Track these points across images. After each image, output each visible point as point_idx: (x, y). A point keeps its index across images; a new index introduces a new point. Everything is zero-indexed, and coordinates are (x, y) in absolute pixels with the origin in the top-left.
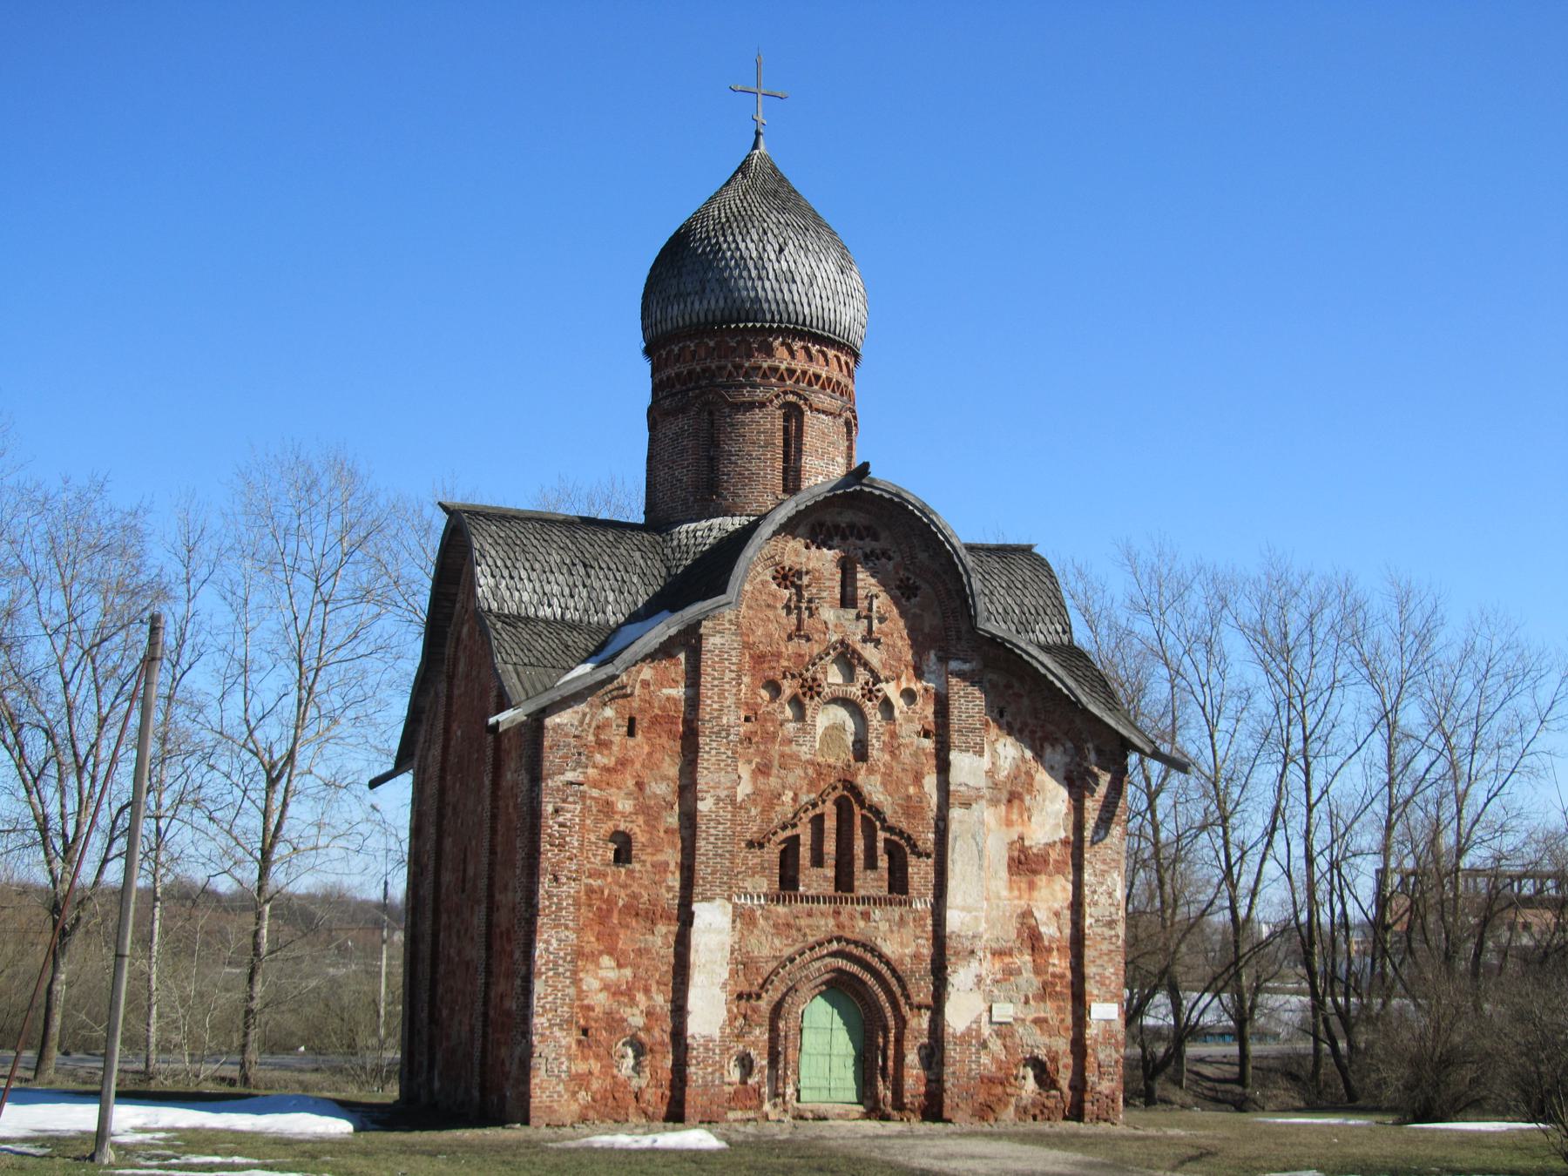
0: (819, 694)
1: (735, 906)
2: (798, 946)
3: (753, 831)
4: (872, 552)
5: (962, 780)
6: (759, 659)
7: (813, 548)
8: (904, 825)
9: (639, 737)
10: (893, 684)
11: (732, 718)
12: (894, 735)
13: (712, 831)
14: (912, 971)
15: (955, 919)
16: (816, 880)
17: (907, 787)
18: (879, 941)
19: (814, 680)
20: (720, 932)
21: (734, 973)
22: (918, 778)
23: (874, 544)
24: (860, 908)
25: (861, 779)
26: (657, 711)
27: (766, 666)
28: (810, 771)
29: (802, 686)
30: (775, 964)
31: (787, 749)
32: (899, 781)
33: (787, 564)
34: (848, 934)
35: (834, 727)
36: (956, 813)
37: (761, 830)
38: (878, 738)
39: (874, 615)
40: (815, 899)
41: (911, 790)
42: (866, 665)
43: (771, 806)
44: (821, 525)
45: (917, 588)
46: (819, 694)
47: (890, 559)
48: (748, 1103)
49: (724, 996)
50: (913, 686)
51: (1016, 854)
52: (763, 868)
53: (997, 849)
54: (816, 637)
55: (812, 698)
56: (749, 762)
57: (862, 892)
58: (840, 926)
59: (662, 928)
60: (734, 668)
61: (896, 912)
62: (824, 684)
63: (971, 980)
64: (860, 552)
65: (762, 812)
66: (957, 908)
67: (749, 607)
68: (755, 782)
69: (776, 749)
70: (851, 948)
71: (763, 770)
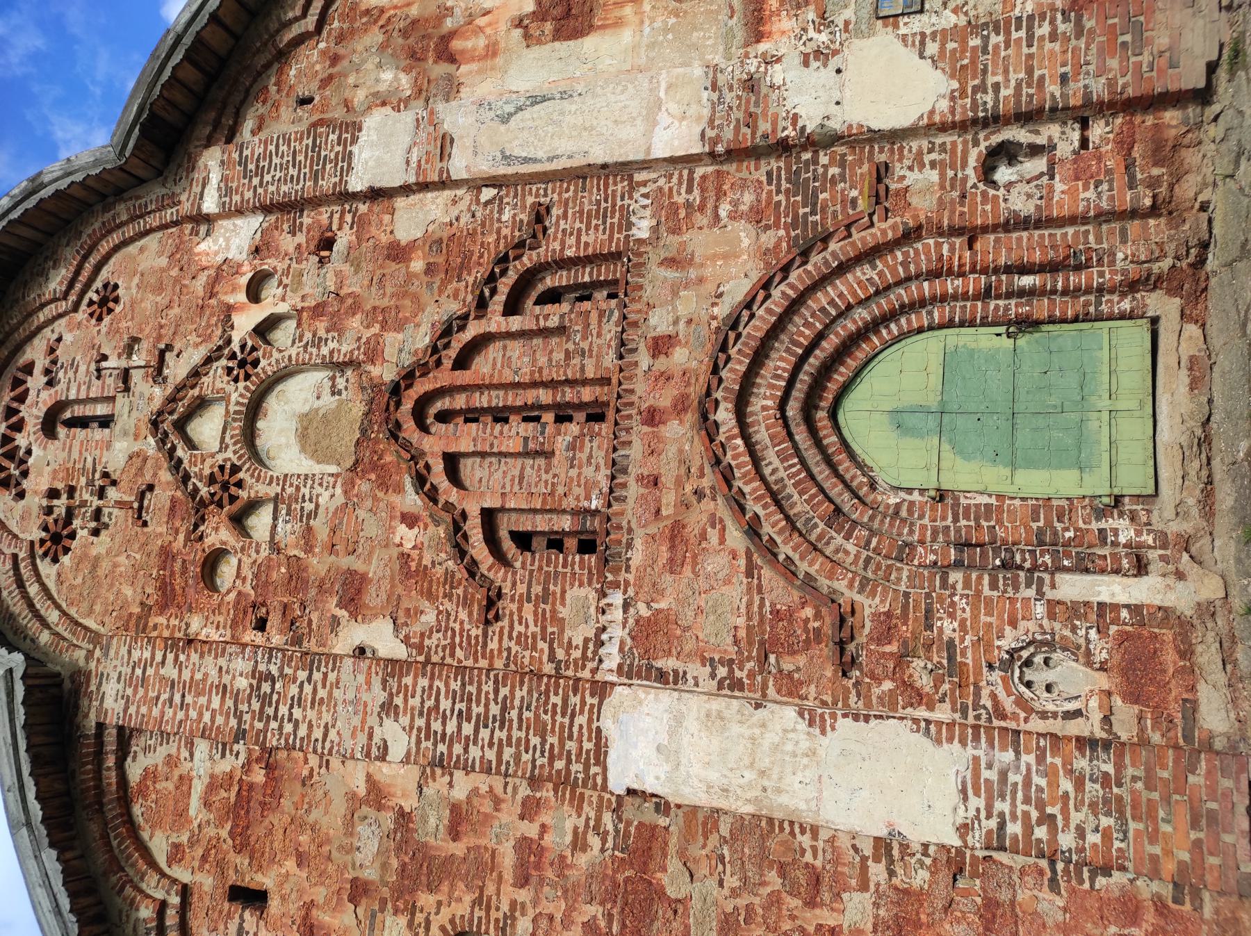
0: (235, 469)
1: (628, 672)
2: (722, 509)
3: (465, 619)
4: (47, 372)
5: (399, 161)
6: (168, 598)
7: (25, 484)
8: (478, 274)
9: (266, 880)
10: (237, 319)
11: (241, 665)
12: (318, 311)
13: (451, 727)
14: (794, 225)
15: (675, 135)
16: (576, 471)
17: (410, 276)
18: (722, 310)
19: (212, 480)
20: (678, 720)
21: (791, 687)
22: (398, 253)
23: (38, 370)
24: (644, 359)
25: (386, 373)
26: (224, 833)
27: (178, 582)
28: (363, 486)
29: (220, 505)
30: (767, 573)
32: (402, 294)
33: (37, 534)
34: (696, 390)
35: (303, 436)
36: (459, 166)
37: (466, 602)
38: (318, 342)
39: (124, 363)
40: (617, 469)
41: (417, 265)
42: (196, 374)
43: (424, 572)
45: (106, 286)
46: (235, 469)
47: (59, 340)
48: (1170, 658)
49: (844, 724)
50: (244, 280)
51: (549, 27)
52: (546, 596)
53: (535, 67)
54: (148, 478)
56: (335, 622)
57: (610, 360)
58: (680, 406)
59: (672, 880)
60: (159, 658)
61: (656, 278)
62: (220, 458)
63: (821, 76)
64: (45, 395)
65: (430, 596)
66: (649, 134)
67: (91, 611)
68: (376, 616)
69: (318, 564)
70: (732, 374)
71: (352, 593)
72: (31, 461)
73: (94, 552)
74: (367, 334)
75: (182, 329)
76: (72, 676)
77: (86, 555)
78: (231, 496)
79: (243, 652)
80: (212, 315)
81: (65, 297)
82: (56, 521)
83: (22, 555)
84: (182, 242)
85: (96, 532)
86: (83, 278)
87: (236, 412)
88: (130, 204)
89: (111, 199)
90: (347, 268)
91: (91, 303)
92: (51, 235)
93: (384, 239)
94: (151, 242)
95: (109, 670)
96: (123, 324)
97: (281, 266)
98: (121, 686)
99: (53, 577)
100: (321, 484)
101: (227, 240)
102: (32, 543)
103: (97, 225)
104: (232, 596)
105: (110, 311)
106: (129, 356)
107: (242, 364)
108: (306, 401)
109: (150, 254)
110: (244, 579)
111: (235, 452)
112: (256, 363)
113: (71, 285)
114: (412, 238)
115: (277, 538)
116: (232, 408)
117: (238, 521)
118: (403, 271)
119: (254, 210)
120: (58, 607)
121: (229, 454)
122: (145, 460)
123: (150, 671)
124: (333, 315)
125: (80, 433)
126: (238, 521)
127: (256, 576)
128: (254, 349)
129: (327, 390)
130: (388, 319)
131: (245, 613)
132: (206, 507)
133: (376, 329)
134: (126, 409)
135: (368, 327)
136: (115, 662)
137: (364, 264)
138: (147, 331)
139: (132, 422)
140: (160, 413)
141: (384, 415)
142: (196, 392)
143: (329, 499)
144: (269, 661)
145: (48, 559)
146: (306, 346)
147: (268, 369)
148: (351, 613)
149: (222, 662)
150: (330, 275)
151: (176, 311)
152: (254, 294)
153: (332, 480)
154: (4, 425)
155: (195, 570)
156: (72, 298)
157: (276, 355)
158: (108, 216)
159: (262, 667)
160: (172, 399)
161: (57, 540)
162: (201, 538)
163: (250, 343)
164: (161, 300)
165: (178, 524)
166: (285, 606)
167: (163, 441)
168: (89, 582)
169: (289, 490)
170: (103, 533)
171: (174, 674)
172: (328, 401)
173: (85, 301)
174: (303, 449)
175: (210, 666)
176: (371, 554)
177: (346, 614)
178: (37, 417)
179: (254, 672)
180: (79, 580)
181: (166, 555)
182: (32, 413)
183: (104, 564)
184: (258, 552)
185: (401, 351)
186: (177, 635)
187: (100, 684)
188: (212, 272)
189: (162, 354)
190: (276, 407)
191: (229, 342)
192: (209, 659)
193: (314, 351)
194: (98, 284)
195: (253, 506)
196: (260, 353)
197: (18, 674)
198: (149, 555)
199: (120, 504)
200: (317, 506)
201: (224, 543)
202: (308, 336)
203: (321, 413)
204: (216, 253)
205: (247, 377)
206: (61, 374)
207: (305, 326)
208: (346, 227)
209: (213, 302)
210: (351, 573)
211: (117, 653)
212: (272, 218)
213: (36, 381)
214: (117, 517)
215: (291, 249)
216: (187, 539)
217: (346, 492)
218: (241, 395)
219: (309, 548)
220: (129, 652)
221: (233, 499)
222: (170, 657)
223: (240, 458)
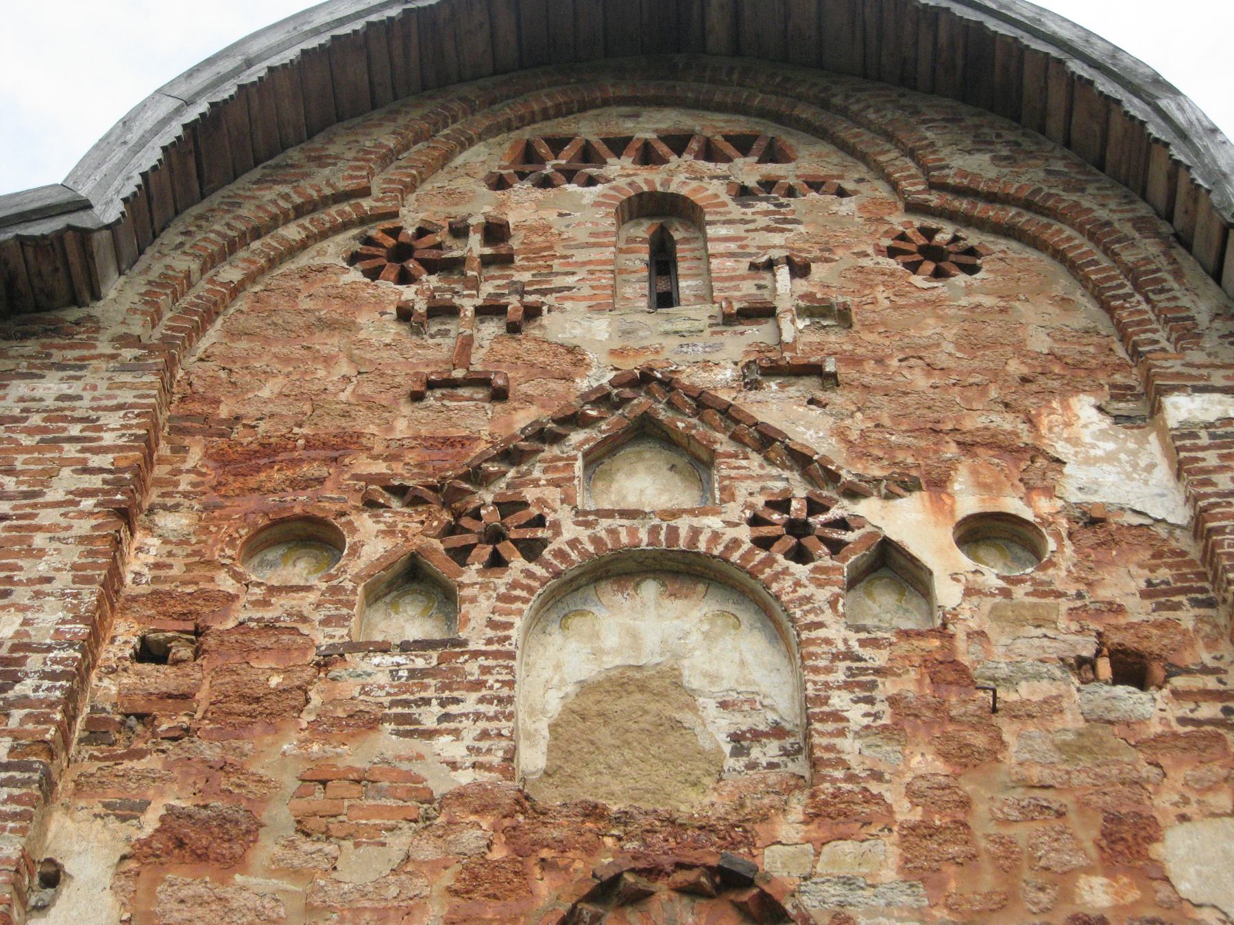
4: (768, 185)
11: (49, 618)
12: (948, 672)
17: (1062, 880)
23: (771, 169)
28: (474, 835)
29: (450, 530)
31: (354, 755)
32: (1009, 859)
33: (409, 222)
35: (625, 682)
38: (862, 684)
42: (767, 441)
44: (557, 144)
45: (971, 252)
46: (531, 549)
47: (842, 193)
50: (1013, 504)
55: (497, 562)
56: (129, 811)
60: (95, 461)
62: (564, 515)
67: (233, 334)
69: (280, 754)
72: (572, 188)
73: (362, 319)
74: (893, 794)
75: (878, 399)
76: (90, 318)
77: (359, 307)
78: (468, 549)
79: (77, 618)
80: (917, 452)
81: (933, 186)
82: (439, 246)
83: (367, 204)
84: (1090, 371)
85: (405, 314)
86: (981, 209)
87: (673, 531)
88: (1162, 261)
89: (1165, 228)
90: (1071, 721)
91: (929, 233)
92: (1068, 144)
93: (1164, 802)
94: (1086, 313)
95: (89, 377)
96: (881, 294)
97: (1059, 576)
98: (50, 403)
99: (318, 261)
100: (485, 735)
101: (1110, 458)
102: (395, 215)
103: (1102, 214)
104: (226, 583)
105: (914, 268)
106: (802, 312)
107: (798, 528)
108: (713, 678)
109: (1047, 313)
110: (265, 603)
111: (574, 543)
112: (800, 555)
113: (959, 191)
114: (1172, 869)
115: (354, 659)
116: (683, 525)
117: (411, 577)
118: (1078, 860)
119: (1192, 499)
120: (251, 278)
121: (570, 530)
122: (567, 378)
123: (71, 450)
124: (939, 708)
125: (639, 259)
126: (411, 577)
127: (269, 627)
128: (836, 547)
129: (744, 723)
130: (935, 843)
131: (184, 616)
132: (446, 505)
133: (907, 813)
134: (682, 326)
135: (912, 793)
136: (102, 388)
137: (1086, 761)
138: (868, 337)
139: (655, 341)
140: (669, 384)
141: (666, 861)
142: (723, 444)
143: (449, 759)
144: (45, 675)
145: (358, 247)
146: (849, 655)
147: (788, 583)
148: (147, 843)
149: (64, 580)
150: (1045, 689)
151: (921, 382)
152: (978, 533)
153: (496, 758)
154: (650, 136)
155: (299, 502)
156: (934, 199)
157: (822, 595)
158: (1128, 229)
159: (34, 662)
160: (702, 402)
161: (395, 255)
162: (371, 504)
163: (849, 536)
164: (947, 354)
165: (411, 457)
166: (185, 697)
167: (603, 399)
168: (300, 321)
169: (473, 669)
170: (403, 329)
171: (55, 493)
172: (717, 729)
173: (932, 223)
174: (585, 688)
175: (56, 558)
176: (295, 873)
177: (148, 830)
178: (666, 183)
179: (28, 647)
180: (305, 303)
181: (339, 447)
182: (679, 176)
183: (335, 340)
184: (326, 622)
185: (848, 882)
186: (154, 496)
187: (61, 367)
188: (1026, 438)
189: (814, 370)
190: (696, 614)
191: (853, 493)
192: (74, 554)
193: (840, 676)
194: (973, 238)
195: (445, 597)
196: (825, 559)
197: (80, 220)
198: (345, 415)
199: (466, 344)
200: (430, 734)
201: (355, 551)
202: (879, 658)
203: (687, 717)
204: (1074, 441)
205: (763, 543)
206: (763, 206)
207: (904, 646)
208: (1185, 709)
209: (951, 451)
210: (252, 832)
211: (123, 385)
212: (1184, 542)
213: (748, 171)
214: (435, 350)
215: (1104, 593)
216: (370, 479)
217: (460, 796)
218: (716, 536)
219: (324, 728)
220: (120, 407)
221: (461, 555)
222: (96, 481)
223: (560, 554)
